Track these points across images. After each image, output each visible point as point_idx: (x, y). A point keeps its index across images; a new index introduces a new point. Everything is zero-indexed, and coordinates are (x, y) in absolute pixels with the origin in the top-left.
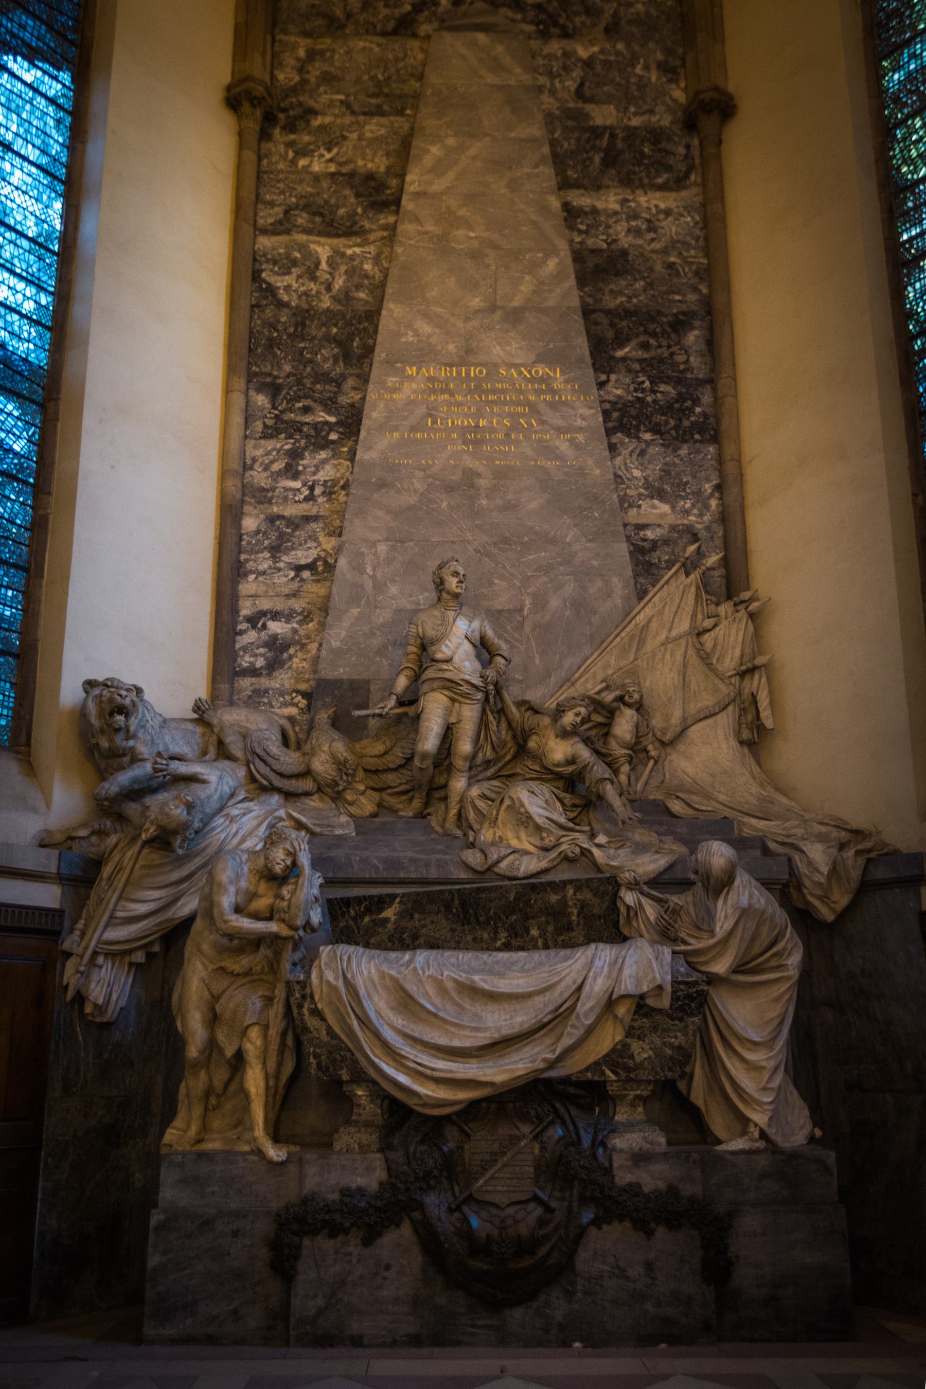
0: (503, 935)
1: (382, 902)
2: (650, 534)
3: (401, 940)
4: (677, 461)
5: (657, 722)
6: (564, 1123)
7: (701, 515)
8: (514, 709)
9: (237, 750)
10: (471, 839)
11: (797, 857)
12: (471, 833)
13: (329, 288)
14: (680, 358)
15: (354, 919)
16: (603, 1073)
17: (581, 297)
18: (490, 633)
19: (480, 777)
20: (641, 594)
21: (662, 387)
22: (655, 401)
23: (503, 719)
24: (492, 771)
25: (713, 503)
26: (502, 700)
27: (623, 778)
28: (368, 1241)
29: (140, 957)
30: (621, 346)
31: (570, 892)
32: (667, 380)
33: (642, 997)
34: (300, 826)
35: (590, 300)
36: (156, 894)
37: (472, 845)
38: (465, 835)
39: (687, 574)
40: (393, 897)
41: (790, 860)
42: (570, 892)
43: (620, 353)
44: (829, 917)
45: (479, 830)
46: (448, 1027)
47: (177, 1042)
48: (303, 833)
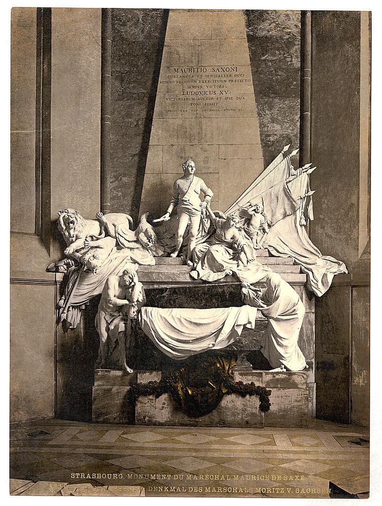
0: (204, 301)
1: (162, 291)
2: (272, 139)
3: (170, 304)
4: (284, 106)
5: (269, 218)
6: (220, 364)
7: (293, 130)
8: (214, 217)
9: (112, 232)
10: (195, 266)
11: (310, 273)
12: (195, 265)
13: (143, 32)
14: (288, 59)
15: (153, 296)
16: (233, 348)
17: (247, 32)
18: (205, 187)
19: (200, 242)
20: (267, 164)
21: (280, 73)
22: (277, 79)
23: (209, 220)
24: (205, 239)
25: (298, 124)
26: (209, 213)
27: (254, 241)
28: (157, 397)
29: (83, 307)
30: (263, 55)
31: (226, 288)
32: (282, 69)
33: (245, 325)
34: (135, 262)
35: (251, 33)
36: (86, 287)
37: (195, 269)
38: (194, 265)
39: (285, 156)
40: (167, 289)
41: (308, 276)
42: (226, 288)
43: (263, 58)
44: (320, 295)
45: (198, 263)
46: (182, 333)
47: (98, 335)
48: (137, 264)
